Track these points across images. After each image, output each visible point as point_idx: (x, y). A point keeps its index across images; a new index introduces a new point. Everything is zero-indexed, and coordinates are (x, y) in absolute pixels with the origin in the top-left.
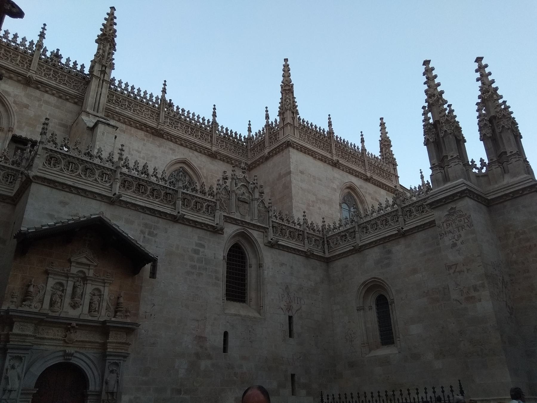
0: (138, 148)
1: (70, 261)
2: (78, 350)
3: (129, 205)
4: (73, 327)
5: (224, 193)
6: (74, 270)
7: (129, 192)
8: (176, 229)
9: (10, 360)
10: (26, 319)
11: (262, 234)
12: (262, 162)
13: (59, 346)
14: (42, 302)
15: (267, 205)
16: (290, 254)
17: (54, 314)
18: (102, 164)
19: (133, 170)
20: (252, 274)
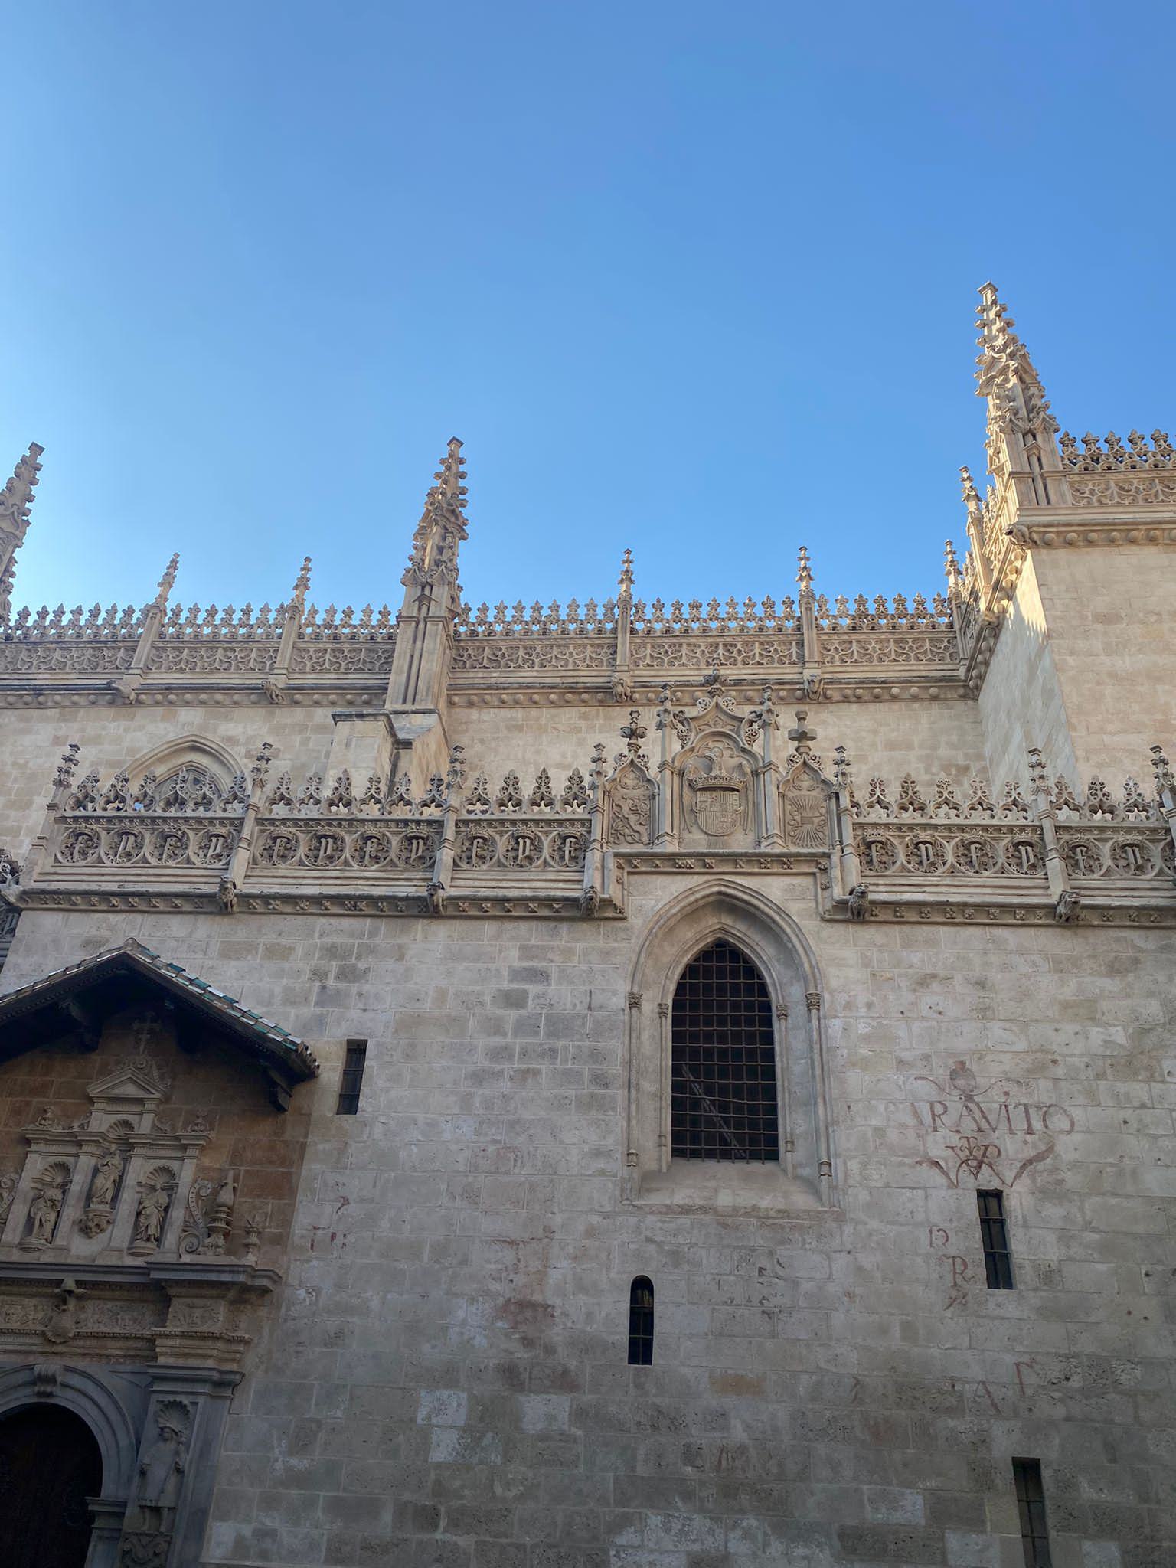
0: (563, 756)
1: (91, 1101)
3: (276, 904)
4: (70, 1292)
5: (630, 783)
6: (102, 1121)
7: (283, 869)
11: (809, 880)
12: (991, 650)
13: (31, 1352)
15: (829, 772)
16: (971, 930)
17: (28, 1258)
18: (210, 814)
19: (302, 802)
20: (790, 1041)
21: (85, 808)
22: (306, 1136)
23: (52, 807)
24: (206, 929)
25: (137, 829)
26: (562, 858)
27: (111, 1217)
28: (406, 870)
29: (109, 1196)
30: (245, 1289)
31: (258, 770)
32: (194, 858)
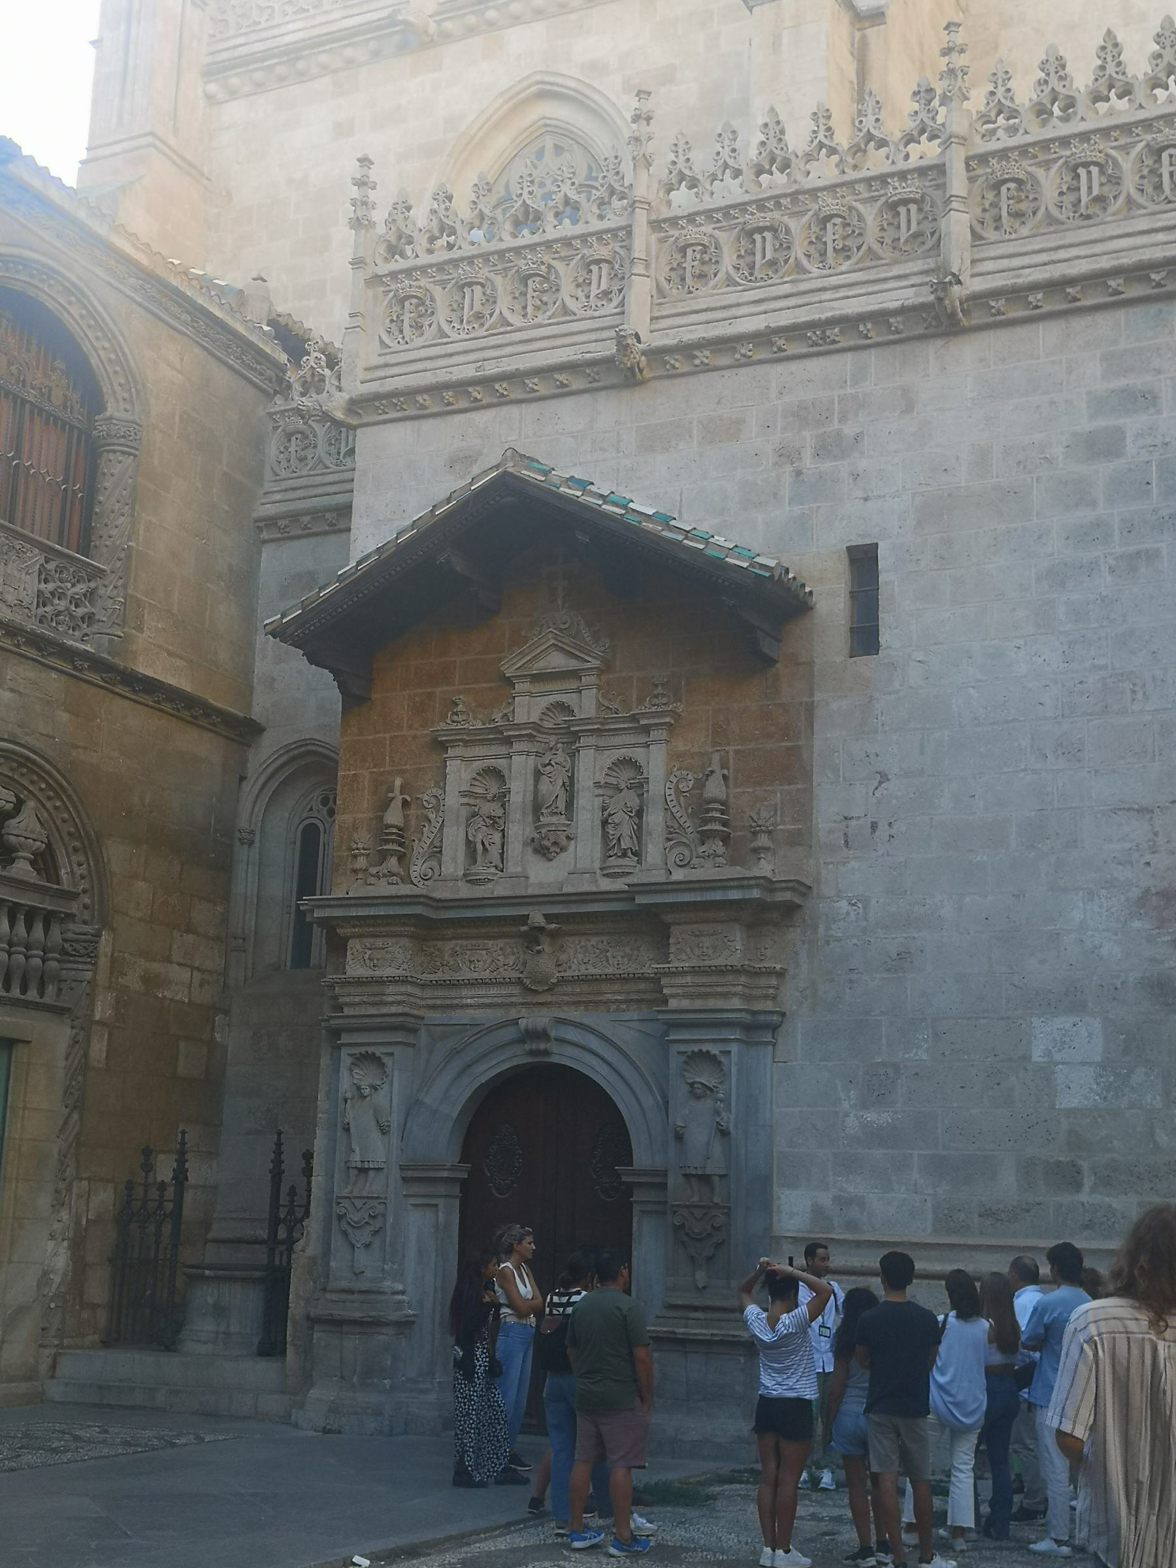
1: (509, 682)
2: (575, 1015)
3: (703, 356)
4: (541, 929)
6: (528, 707)
8: (967, 363)
9: (351, 1070)
10: (378, 925)
13: (512, 1004)
14: (436, 852)
17: (478, 892)
18: (579, 229)
19: (713, 178)
21: (402, 255)
22: (812, 695)
23: (358, 263)
24: (611, 414)
25: (484, 273)
26: (1159, 187)
27: (569, 832)
28: (896, 262)
29: (562, 806)
30: (762, 907)
31: (637, 139)
32: (572, 304)
